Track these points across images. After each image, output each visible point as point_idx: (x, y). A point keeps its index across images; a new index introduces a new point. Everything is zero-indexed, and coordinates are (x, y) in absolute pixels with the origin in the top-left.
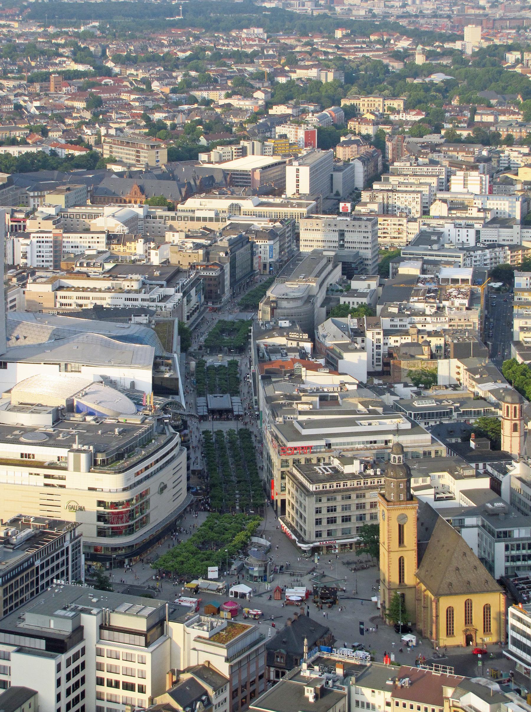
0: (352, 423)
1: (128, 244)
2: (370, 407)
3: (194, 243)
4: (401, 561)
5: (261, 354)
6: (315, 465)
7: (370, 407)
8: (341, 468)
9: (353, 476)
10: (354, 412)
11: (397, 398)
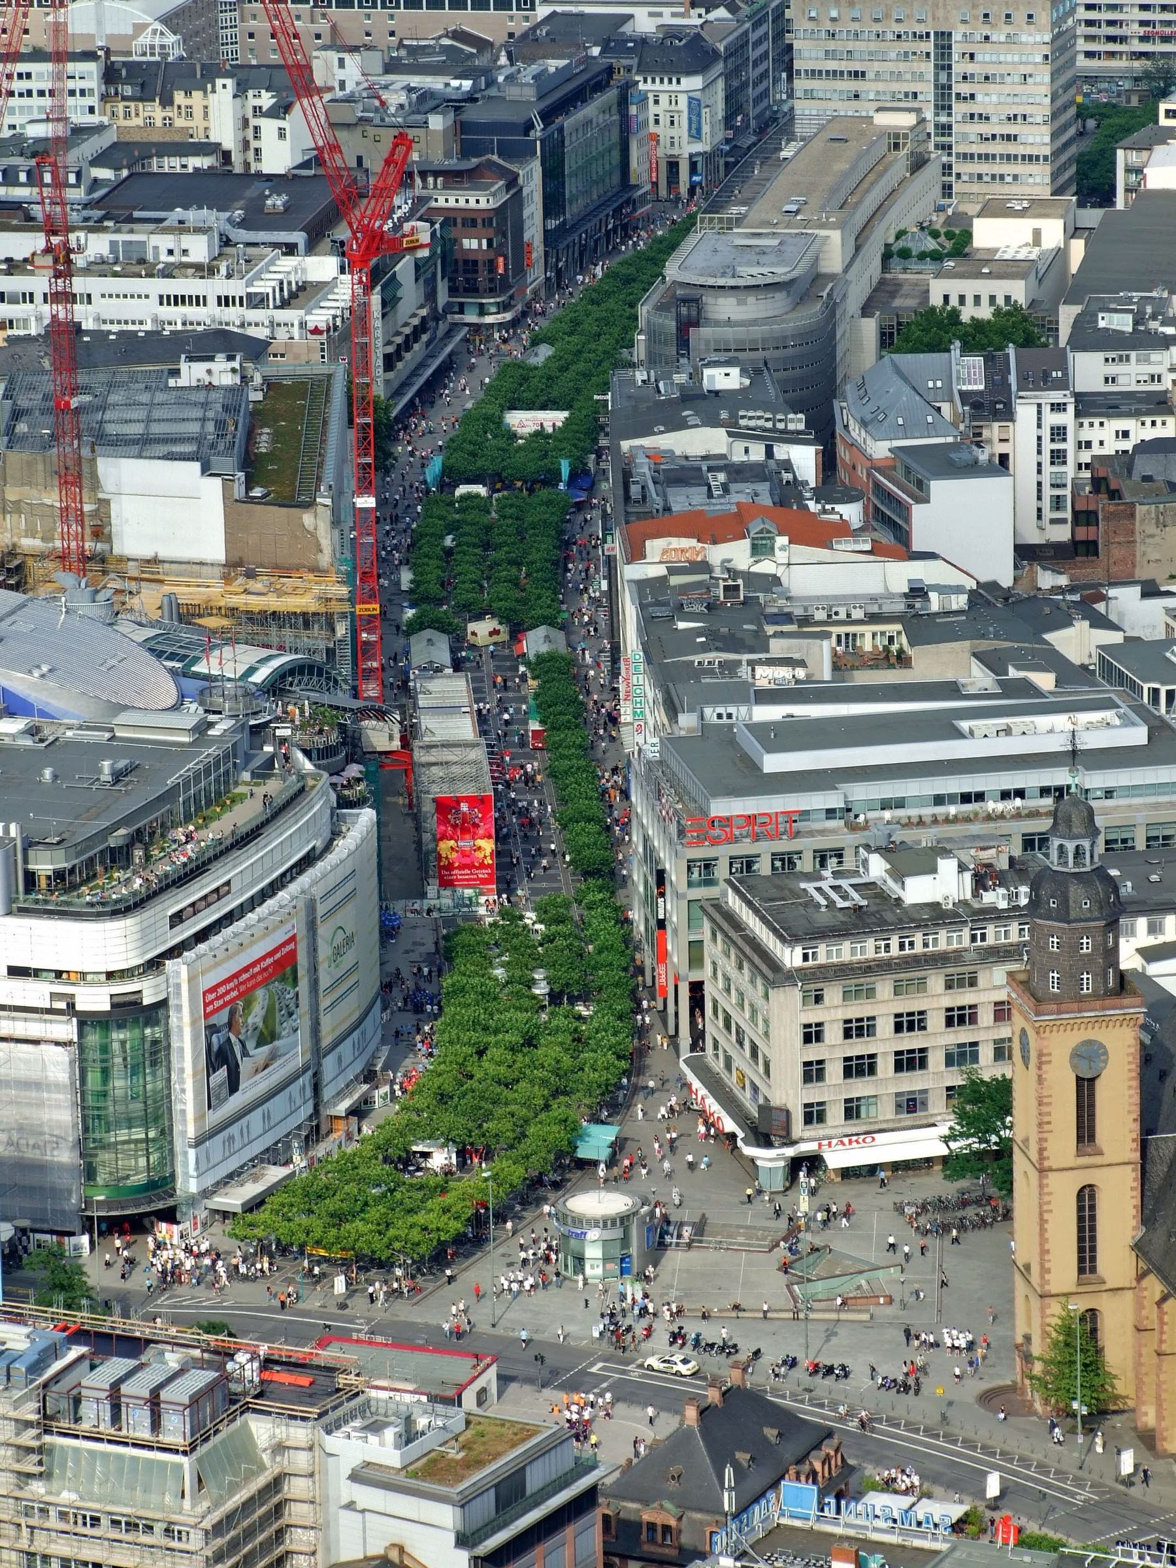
0: (943, 727)
1: (179, 97)
2: (1013, 673)
3: (410, 90)
4: (1086, 1199)
5: (635, 490)
6: (809, 877)
7: (1013, 673)
8: (892, 886)
9: (936, 916)
10: (951, 690)
11: (1116, 638)
